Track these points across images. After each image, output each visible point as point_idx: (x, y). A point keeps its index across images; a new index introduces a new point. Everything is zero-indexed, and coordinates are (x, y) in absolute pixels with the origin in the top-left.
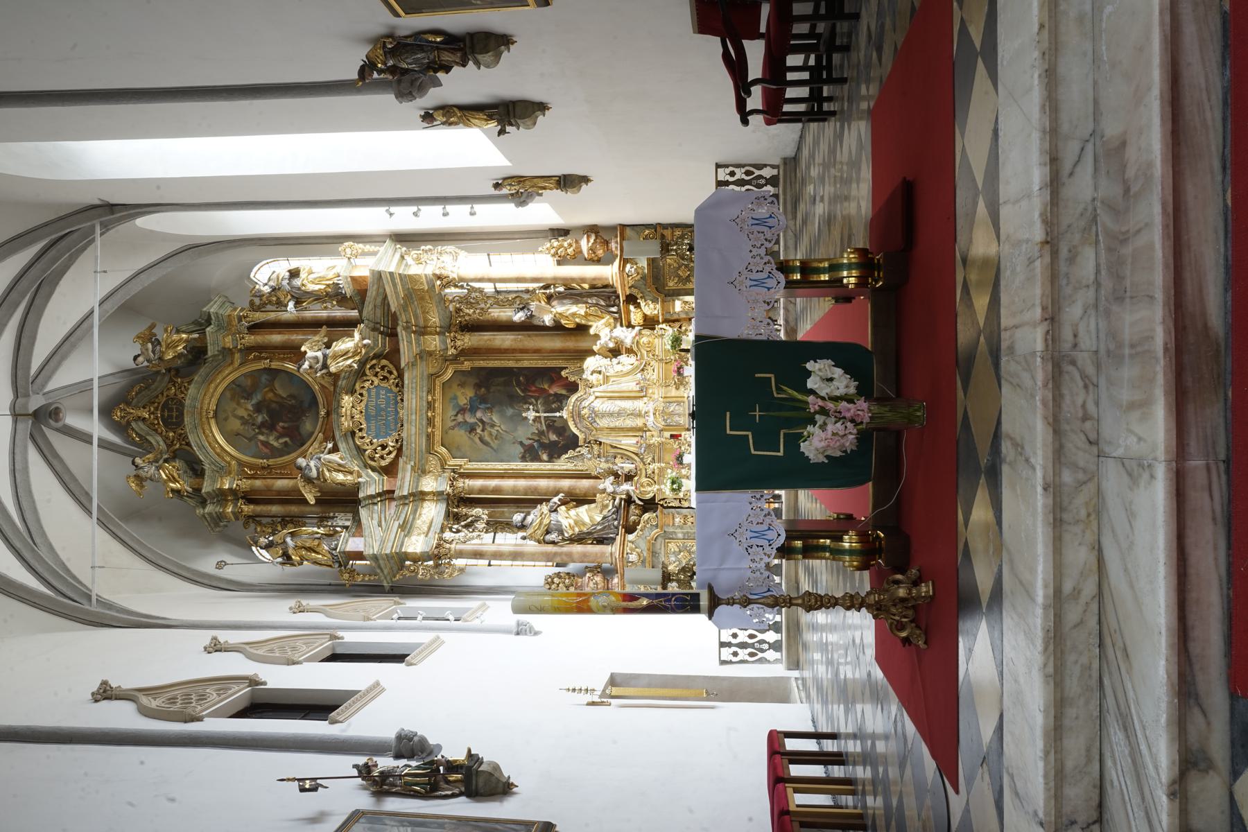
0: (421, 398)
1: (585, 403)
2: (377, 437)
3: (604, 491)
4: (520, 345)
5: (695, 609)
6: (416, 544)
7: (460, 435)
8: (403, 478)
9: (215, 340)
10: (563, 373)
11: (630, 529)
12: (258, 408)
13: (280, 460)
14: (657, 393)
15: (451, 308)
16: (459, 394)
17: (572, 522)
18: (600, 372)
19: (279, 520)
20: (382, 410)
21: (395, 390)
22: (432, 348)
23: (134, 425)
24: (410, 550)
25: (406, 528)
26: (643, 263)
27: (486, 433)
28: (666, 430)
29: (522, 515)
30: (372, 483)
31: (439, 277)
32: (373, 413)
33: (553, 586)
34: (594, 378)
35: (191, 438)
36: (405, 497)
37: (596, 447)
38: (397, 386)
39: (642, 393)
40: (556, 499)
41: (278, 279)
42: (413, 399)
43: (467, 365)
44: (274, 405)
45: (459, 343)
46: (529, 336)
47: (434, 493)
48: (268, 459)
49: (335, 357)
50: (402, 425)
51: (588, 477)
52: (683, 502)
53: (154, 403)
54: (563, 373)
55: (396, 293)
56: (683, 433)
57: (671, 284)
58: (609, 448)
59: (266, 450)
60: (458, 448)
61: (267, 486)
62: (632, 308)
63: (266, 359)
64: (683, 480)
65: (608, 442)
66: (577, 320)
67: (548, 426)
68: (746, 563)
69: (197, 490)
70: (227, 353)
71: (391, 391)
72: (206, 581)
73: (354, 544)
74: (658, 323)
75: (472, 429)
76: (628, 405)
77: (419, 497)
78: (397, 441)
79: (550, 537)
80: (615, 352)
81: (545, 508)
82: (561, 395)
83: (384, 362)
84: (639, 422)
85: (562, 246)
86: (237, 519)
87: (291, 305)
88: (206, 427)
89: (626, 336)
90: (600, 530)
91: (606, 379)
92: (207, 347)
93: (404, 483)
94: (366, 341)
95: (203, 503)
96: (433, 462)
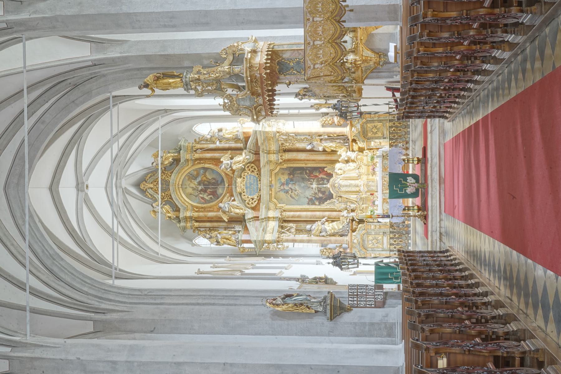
0: (267, 179)
1: (337, 182)
2: (250, 195)
3: (343, 216)
4: (308, 158)
5: (389, 217)
6: (268, 237)
7: (282, 195)
8: (262, 211)
9: (184, 156)
10: (325, 169)
11: (354, 231)
12: (199, 184)
13: (209, 205)
14: (364, 177)
15: (280, 143)
16: (281, 178)
17: (331, 228)
18: (340, 169)
19: (208, 229)
20: (252, 184)
21: (257, 176)
22: (272, 159)
23: (148, 190)
24: (267, 239)
25: (264, 230)
26: (359, 126)
27: (293, 194)
28: (368, 192)
29: (310, 226)
30: (250, 214)
31: (278, 132)
32: (248, 186)
33: (324, 253)
34: (339, 172)
35: (173, 196)
36: (262, 219)
37: (340, 199)
38: (257, 174)
39: (359, 177)
40: (324, 219)
41: (214, 132)
42: (265, 180)
43: (285, 166)
44: (206, 182)
45: (283, 157)
46: (312, 154)
47: (274, 218)
48: (204, 204)
49: (235, 163)
50: (260, 190)
51: (336, 211)
52: (374, 220)
53: (156, 181)
54: (325, 169)
55: (261, 138)
56: (375, 193)
57: (370, 135)
58: (345, 199)
59: (203, 201)
60: (281, 200)
61: (205, 215)
62: (354, 144)
63: (203, 163)
64: (375, 211)
65: (345, 197)
66: (332, 149)
67: (319, 191)
68: (398, 212)
69: (178, 217)
70: (187, 161)
71: (255, 176)
72: (182, 253)
73: (245, 237)
74: (365, 150)
75: (287, 192)
76: (353, 182)
77: (268, 219)
78: (258, 197)
79: (323, 234)
80: (347, 162)
81: (319, 223)
82: (324, 178)
83: (253, 165)
84: (357, 189)
85: (327, 120)
86: (192, 228)
87: (218, 143)
88: (178, 191)
89: (352, 155)
90: (342, 232)
91: (344, 172)
92: (180, 159)
93: (262, 213)
94: (247, 157)
95: (179, 221)
96: (272, 205)
